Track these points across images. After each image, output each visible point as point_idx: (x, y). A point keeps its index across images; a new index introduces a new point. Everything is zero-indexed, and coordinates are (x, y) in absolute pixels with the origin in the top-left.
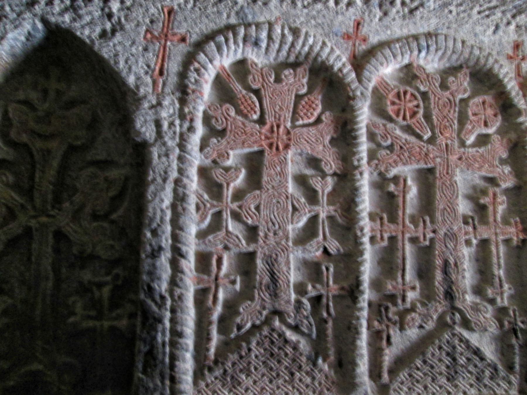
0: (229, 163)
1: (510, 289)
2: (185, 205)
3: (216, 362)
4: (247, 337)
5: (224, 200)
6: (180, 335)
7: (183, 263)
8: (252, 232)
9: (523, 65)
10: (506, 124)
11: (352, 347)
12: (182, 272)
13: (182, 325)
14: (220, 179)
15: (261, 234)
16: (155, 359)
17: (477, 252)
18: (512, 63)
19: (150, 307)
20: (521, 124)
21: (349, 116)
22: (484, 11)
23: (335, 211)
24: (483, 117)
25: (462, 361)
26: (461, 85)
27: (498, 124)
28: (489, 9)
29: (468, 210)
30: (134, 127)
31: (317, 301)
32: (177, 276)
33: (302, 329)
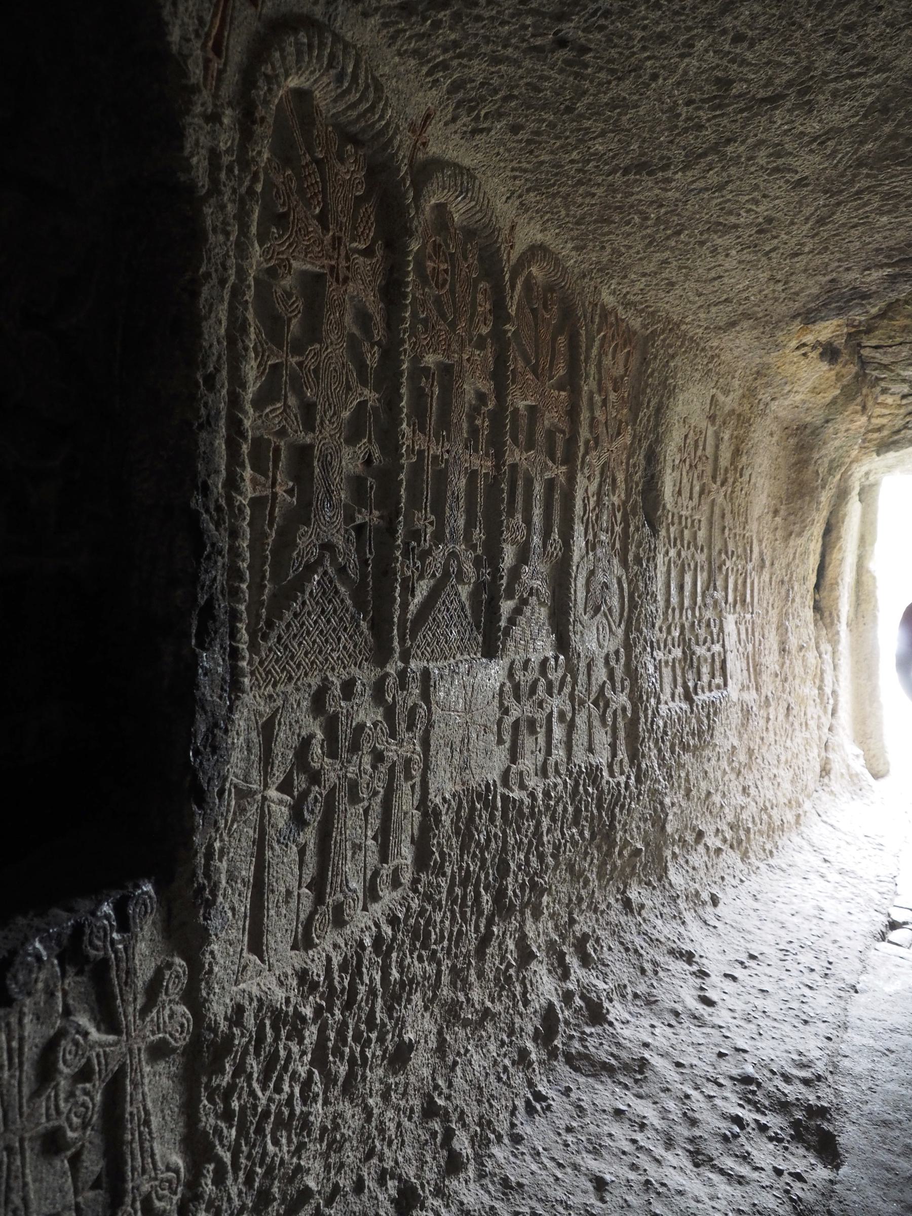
25: (455, 618)
30: (181, 148)
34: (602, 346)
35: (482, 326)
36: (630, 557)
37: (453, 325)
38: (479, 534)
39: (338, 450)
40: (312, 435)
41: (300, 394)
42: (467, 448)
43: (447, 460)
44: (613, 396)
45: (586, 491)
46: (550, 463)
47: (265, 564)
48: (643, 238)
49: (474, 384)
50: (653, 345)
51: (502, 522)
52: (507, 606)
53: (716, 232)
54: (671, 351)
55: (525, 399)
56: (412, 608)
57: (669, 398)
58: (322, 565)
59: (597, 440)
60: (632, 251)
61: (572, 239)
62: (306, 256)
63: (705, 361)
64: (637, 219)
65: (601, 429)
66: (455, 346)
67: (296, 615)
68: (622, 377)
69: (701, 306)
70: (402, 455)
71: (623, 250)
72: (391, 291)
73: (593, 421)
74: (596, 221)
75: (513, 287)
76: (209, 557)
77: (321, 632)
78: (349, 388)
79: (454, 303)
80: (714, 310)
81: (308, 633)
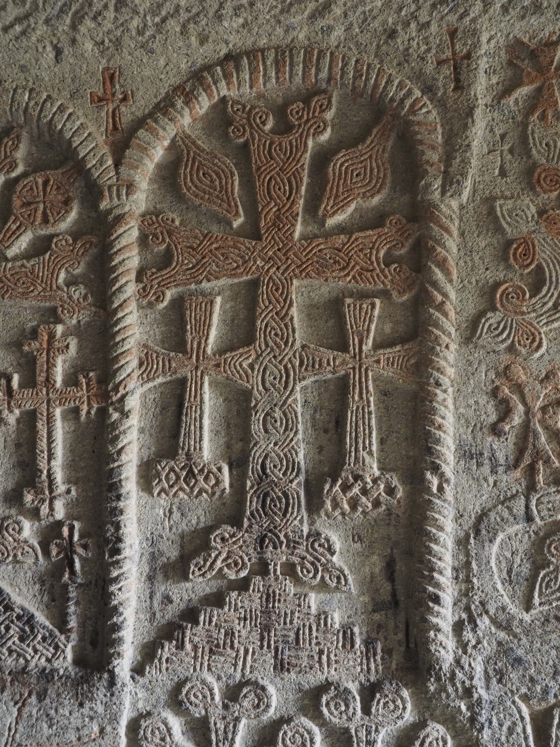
1: (68, 492)
9: (123, 109)
10: (94, 214)
17: (19, 431)
18: (100, 108)
20: (109, 211)
22: (12, 26)
24: (41, 206)
26: (6, 157)
27: (73, 215)
28: (18, 20)
29: (6, 365)
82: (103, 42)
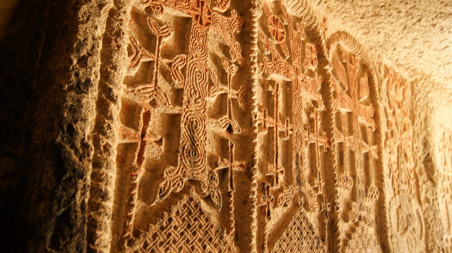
0: (160, 17)
2: (120, 42)
3: (137, 234)
4: (167, 206)
5: (156, 53)
6: (104, 197)
7: (113, 107)
8: (178, 96)
11: (247, 219)
12: (111, 118)
13: (106, 184)
14: (154, 30)
15: (185, 98)
16: (71, 226)
19: (70, 154)
20: (326, 70)
21: (248, 20)
23: (237, 95)
25: (305, 234)
31: (223, 173)
32: (104, 123)
33: (214, 200)
34: (388, 85)
35: (310, 65)
36: (422, 198)
37: (290, 61)
38: (320, 182)
39: (203, 119)
40: (179, 108)
41: (170, 81)
42: (306, 129)
43: (291, 135)
44: (398, 111)
45: (390, 160)
46: (364, 144)
47: (132, 189)
48: (401, 24)
49: (307, 95)
50: (417, 85)
51: (335, 175)
52: (343, 227)
53: (441, 18)
54: (428, 89)
55: (344, 107)
56: (270, 225)
57: (431, 113)
58: (188, 193)
59: (392, 132)
60: (396, 33)
61: (361, 28)
62: (175, 5)
63: (447, 95)
64: (395, 13)
65: (394, 127)
66: (292, 72)
67: (162, 228)
68: (402, 102)
69: (440, 66)
70: (255, 128)
71: (391, 33)
72: (245, 36)
73: (388, 124)
74: (372, 16)
75: (328, 48)
76: (69, 179)
77: (188, 241)
78: (211, 84)
79: (290, 50)
80: (447, 67)
81: (175, 242)
82: (329, 8)
